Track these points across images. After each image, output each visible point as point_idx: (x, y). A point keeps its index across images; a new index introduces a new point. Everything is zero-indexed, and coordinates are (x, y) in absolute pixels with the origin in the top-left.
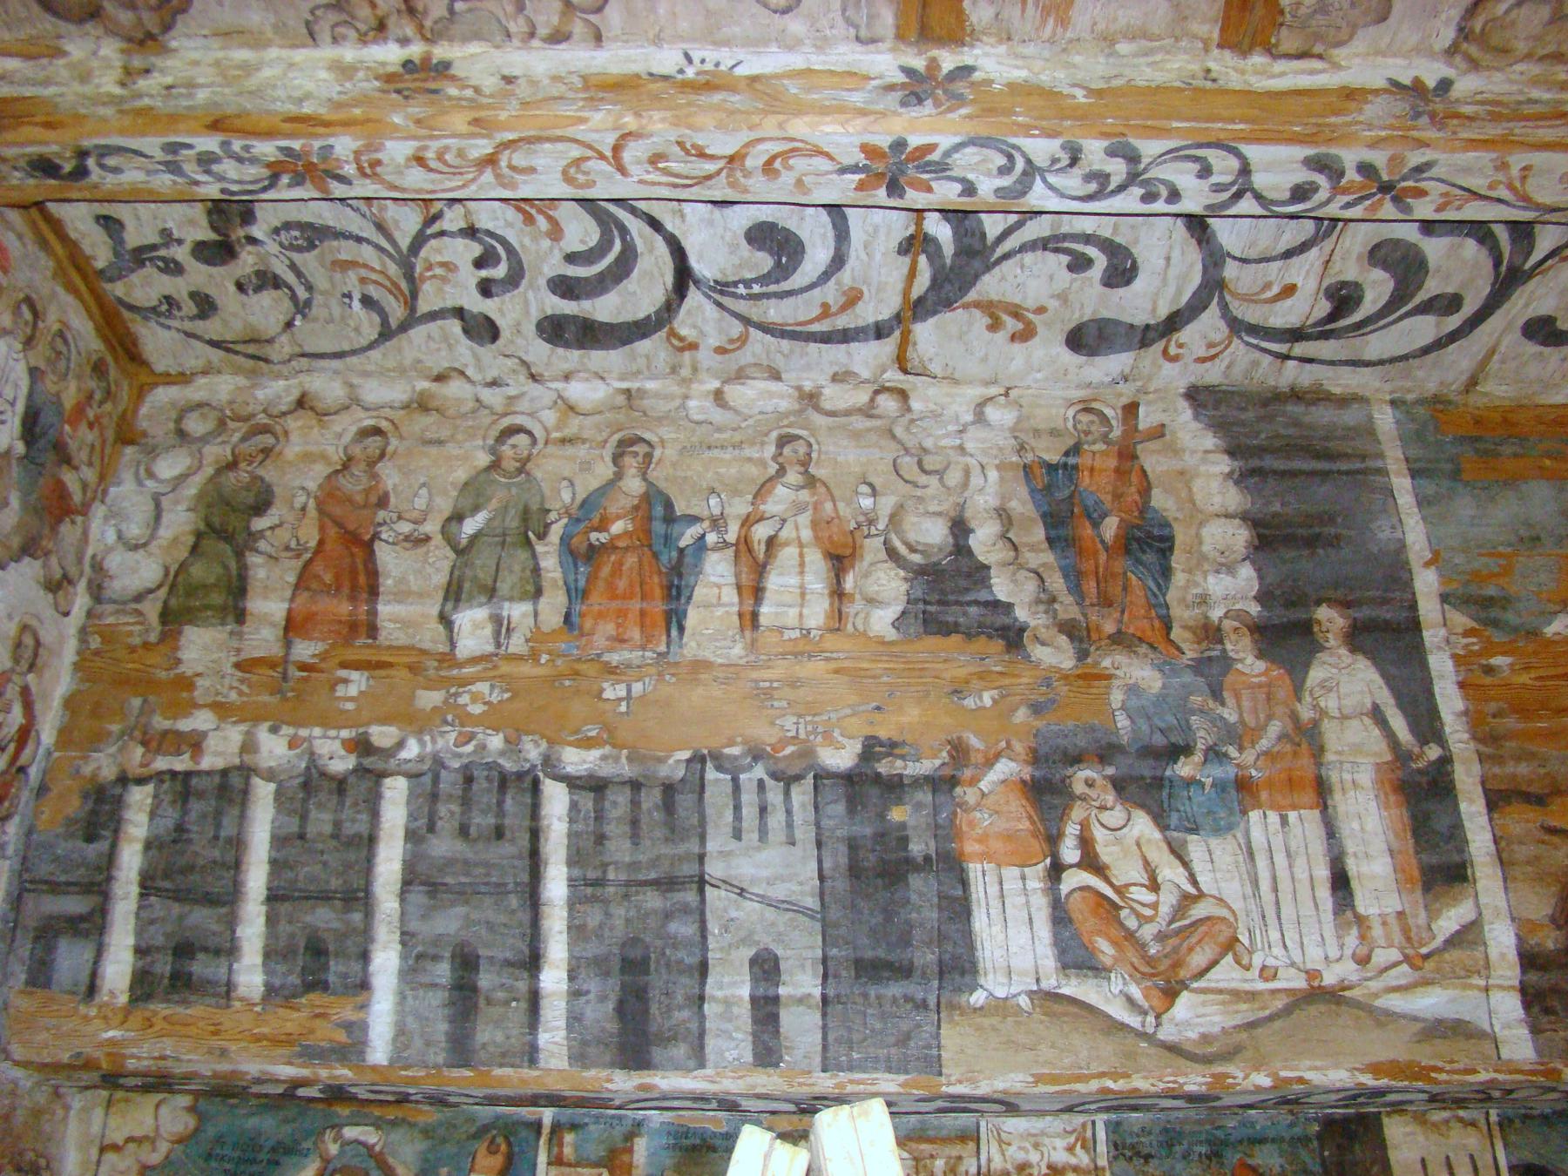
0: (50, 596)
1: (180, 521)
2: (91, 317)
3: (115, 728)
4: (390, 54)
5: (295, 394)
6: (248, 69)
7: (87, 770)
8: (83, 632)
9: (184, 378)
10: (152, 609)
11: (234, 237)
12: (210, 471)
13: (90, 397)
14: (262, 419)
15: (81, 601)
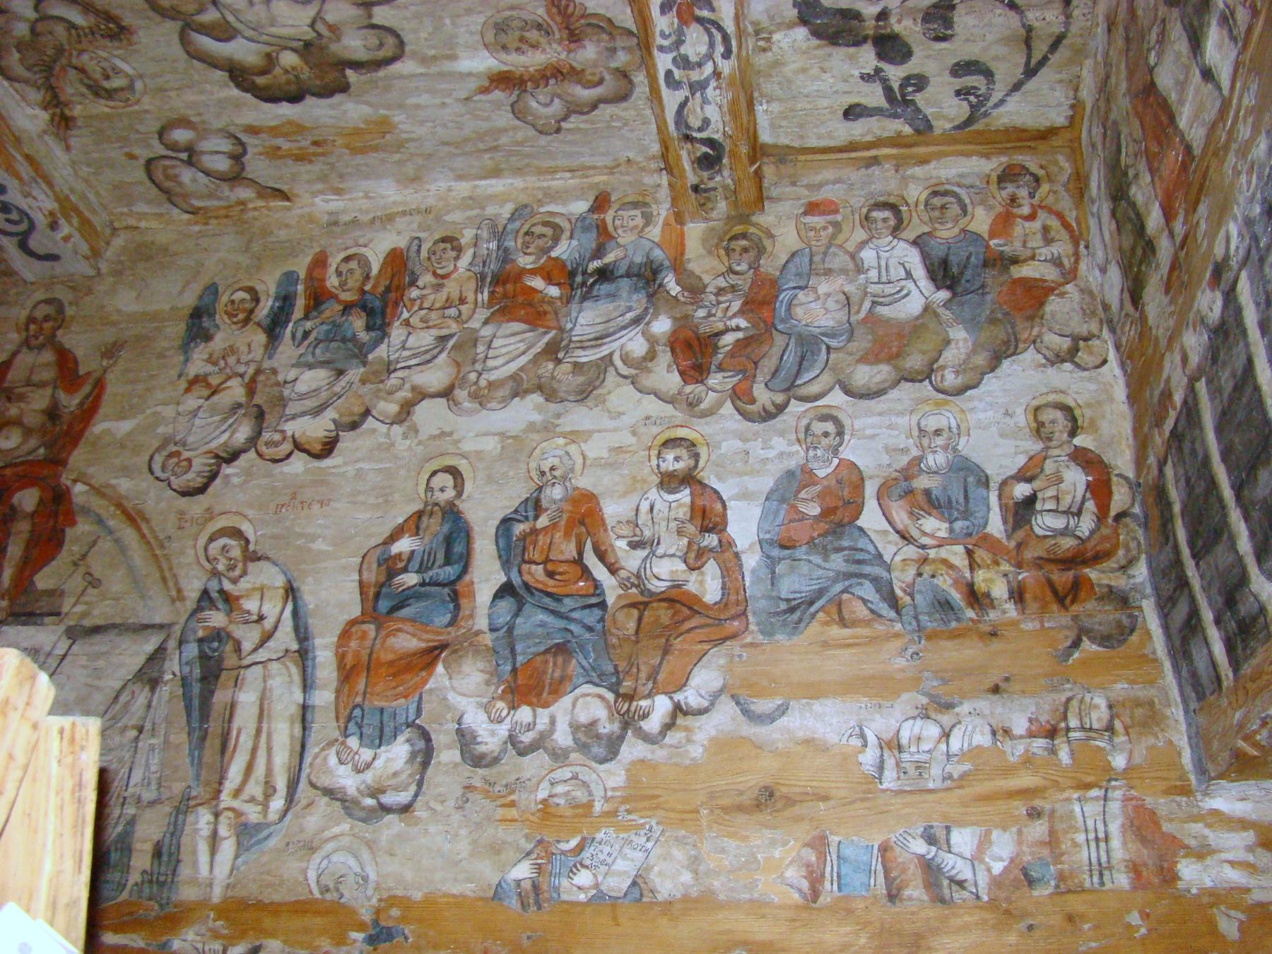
0: (1068, 366)
2: (968, 155)
8: (1122, 365)
11: (871, 32)
13: (1013, 199)
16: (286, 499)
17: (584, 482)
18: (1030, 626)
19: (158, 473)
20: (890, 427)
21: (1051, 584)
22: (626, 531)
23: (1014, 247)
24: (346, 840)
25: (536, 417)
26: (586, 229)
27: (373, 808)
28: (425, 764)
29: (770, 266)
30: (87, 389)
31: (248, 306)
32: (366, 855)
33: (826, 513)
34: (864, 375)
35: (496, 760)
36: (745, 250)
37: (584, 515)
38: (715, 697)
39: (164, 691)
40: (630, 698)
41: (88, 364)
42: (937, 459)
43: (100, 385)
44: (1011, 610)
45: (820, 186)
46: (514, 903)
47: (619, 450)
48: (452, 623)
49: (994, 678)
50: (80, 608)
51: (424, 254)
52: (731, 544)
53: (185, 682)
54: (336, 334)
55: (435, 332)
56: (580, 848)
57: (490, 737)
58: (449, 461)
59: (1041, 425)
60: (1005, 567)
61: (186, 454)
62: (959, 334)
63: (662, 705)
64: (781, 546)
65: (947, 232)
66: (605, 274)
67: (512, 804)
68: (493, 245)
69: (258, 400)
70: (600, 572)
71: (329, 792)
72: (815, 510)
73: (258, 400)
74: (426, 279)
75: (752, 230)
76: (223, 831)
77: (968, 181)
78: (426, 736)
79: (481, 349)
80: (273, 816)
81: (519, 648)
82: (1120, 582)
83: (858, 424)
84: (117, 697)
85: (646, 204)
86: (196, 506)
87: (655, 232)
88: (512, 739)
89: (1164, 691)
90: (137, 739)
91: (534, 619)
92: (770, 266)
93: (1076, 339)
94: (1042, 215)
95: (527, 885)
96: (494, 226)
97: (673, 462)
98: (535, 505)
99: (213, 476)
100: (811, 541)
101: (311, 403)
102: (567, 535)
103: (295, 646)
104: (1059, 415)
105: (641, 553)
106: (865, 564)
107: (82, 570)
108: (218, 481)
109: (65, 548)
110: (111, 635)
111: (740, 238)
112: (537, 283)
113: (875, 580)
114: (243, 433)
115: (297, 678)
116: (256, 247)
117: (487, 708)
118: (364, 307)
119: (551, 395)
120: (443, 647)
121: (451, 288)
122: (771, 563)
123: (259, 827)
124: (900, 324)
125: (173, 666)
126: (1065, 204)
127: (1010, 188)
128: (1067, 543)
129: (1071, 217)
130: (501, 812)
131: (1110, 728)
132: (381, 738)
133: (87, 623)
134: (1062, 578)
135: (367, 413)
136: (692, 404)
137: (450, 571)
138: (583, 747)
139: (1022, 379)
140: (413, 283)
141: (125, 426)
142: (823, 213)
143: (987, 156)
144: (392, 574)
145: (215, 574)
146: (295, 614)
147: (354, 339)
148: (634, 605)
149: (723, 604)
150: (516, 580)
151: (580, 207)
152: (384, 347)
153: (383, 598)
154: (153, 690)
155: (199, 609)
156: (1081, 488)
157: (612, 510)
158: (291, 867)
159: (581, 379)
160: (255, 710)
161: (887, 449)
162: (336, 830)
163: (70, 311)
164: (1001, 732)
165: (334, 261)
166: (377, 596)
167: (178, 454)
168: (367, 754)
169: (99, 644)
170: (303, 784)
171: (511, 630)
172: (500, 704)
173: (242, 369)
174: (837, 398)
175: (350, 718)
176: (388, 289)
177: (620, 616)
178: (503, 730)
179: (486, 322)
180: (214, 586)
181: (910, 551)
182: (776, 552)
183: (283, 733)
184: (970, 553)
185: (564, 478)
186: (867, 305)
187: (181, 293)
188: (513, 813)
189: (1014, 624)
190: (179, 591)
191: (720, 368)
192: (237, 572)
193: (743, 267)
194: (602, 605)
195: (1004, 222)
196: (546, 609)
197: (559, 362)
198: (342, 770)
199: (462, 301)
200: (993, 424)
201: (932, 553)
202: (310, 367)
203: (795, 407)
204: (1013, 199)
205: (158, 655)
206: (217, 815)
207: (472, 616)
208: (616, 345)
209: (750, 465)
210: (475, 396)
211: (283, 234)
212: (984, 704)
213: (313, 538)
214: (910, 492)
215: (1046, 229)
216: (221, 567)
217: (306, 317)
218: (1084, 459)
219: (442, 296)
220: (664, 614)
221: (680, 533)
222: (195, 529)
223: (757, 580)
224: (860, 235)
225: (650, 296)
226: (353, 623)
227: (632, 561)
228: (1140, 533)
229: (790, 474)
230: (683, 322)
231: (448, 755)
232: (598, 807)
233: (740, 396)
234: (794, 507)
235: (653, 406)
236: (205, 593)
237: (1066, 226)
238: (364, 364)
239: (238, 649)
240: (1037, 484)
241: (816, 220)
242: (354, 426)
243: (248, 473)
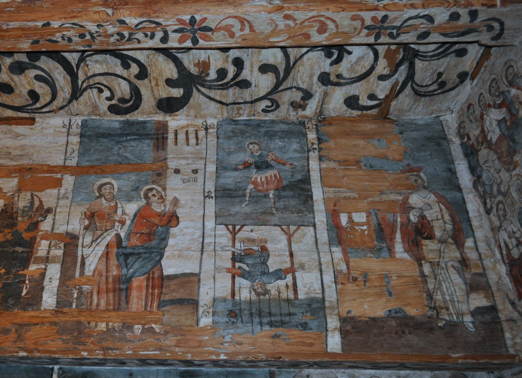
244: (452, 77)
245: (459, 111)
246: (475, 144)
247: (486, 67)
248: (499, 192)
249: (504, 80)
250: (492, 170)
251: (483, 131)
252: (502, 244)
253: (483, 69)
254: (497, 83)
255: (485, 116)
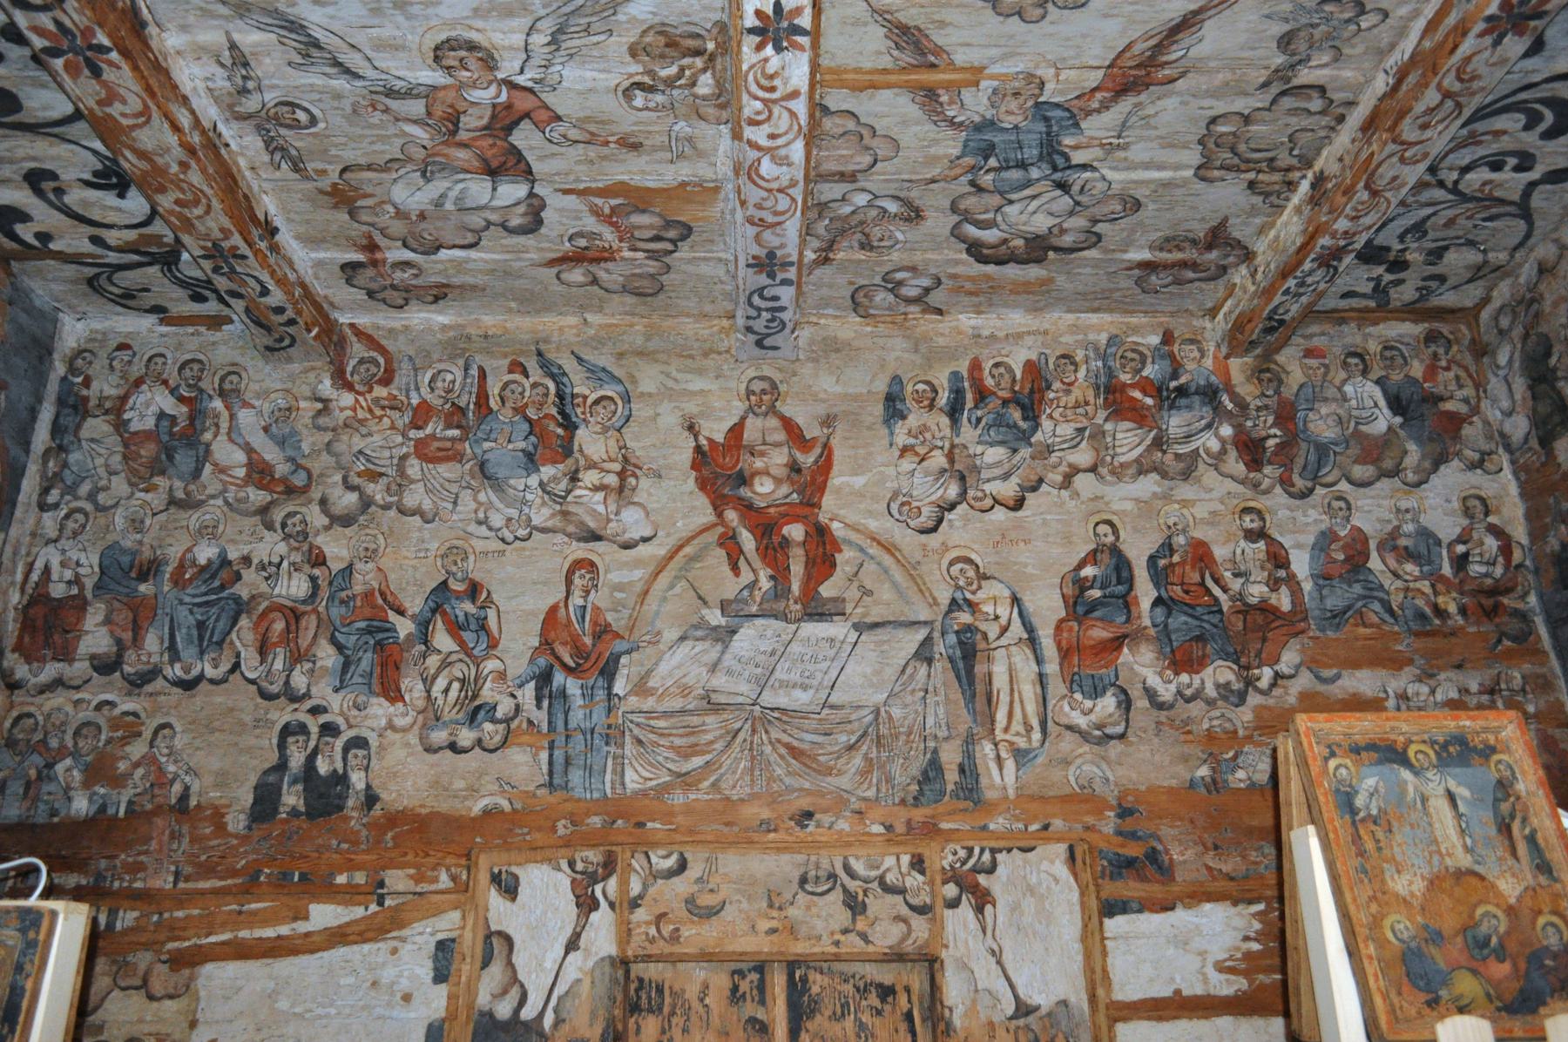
0: (1479, 471)
1: (1520, 385)
2: (1404, 320)
3: (1548, 520)
4: (1305, 186)
5: (1536, 266)
6: (1277, 238)
7: (1548, 550)
8: (1515, 473)
9: (1486, 300)
10: (1534, 443)
12: (1519, 346)
13: (1435, 356)
14: (1528, 296)
15: (1504, 459)
16: (999, 538)
17: (1198, 534)
18: (1472, 629)
19: (897, 516)
20: (1379, 506)
21: (1481, 606)
22: (1229, 566)
23: (1439, 390)
24: (1089, 757)
25: (1159, 490)
26: (1162, 357)
27: (1101, 737)
28: (1128, 709)
29: (1289, 392)
30: (818, 450)
31: (930, 395)
32: (1104, 766)
33: (1347, 560)
34: (1359, 471)
35: (1172, 706)
36: (1270, 380)
37: (1201, 554)
38: (1298, 667)
39: (938, 665)
40: (1248, 668)
41: (812, 431)
42: (1409, 528)
43: (826, 446)
44: (1460, 621)
45: (1312, 336)
46: (1203, 790)
47: (1214, 513)
48: (1128, 620)
49: (1456, 659)
50: (859, 610)
51: (1051, 366)
52: (1294, 576)
53: (951, 660)
54: (999, 422)
55: (1073, 425)
56: (1235, 757)
57: (1166, 692)
58: (1105, 517)
59: (1467, 508)
60: (1454, 595)
61: (915, 504)
62: (1412, 447)
63: (1267, 673)
64: (1323, 578)
65: (1396, 376)
66: (1182, 391)
67: (1189, 732)
68: (1100, 364)
69: (957, 467)
70: (1217, 591)
71: (1069, 728)
72: (1342, 557)
73: (957, 467)
74: (1057, 385)
75: (1272, 366)
76: (1004, 754)
77: (1406, 340)
78: (1124, 692)
79: (1109, 439)
80: (1035, 744)
81: (1173, 637)
82: (1520, 606)
83: (1359, 503)
84: (903, 671)
85: (1199, 342)
86: (933, 540)
87: (1209, 362)
88: (1179, 693)
89: (1552, 670)
90: (924, 698)
91: (1179, 620)
92: (1289, 392)
93: (1483, 453)
94: (1454, 367)
95: (1208, 780)
96: (1096, 349)
97: (1249, 522)
98: (1168, 547)
99: (940, 521)
100: (1340, 576)
101: (997, 472)
102: (1193, 567)
103: (1025, 636)
104: (1477, 503)
105: (1241, 580)
106: (1373, 590)
107: (856, 584)
108: (944, 524)
109: (838, 568)
110: (889, 629)
111: (1266, 372)
112: (1137, 394)
113: (1381, 601)
114: (953, 491)
115: (1031, 656)
116: (923, 348)
117: (1160, 674)
118: (1018, 404)
119: (1164, 475)
120: (1125, 636)
121: (1077, 393)
122: (1319, 588)
123: (1027, 752)
124: (1375, 438)
125: (940, 648)
126: (1468, 359)
127: (1433, 348)
128: (1489, 581)
129: (1473, 369)
130: (1183, 737)
131: (1523, 690)
132: (1096, 692)
133: (868, 620)
134: (1488, 602)
135: (1041, 481)
136: (1256, 486)
137: (1121, 589)
138: (1225, 698)
139: (1452, 479)
140: (1049, 387)
141: (859, 481)
142: (1317, 357)
143: (1416, 322)
144: (1083, 589)
145: (958, 587)
146: (1021, 614)
147: (1015, 426)
148: (1238, 612)
149: (1293, 612)
150: (1164, 594)
151: (1155, 340)
152: (1039, 433)
153: (1078, 605)
154: (930, 665)
155: (950, 611)
156: (1495, 549)
157: (1220, 552)
158: (1056, 774)
159: (1182, 465)
160: (1006, 677)
161: (1379, 520)
162: (1081, 751)
163: (783, 388)
164: (1464, 691)
165: (987, 366)
166: (1075, 603)
167: (909, 503)
168: (1088, 704)
169: (881, 634)
170: (1050, 723)
171: (1166, 626)
172: (1168, 672)
173: (940, 444)
174: (1344, 486)
175: (1073, 682)
176: (1032, 391)
177: (1233, 619)
178: (1173, 688)
179: (1106, 420)
180: (958, 595)
181: (1399, 584)
182: (1321, 582)
183: (1029, 691)
184: (1433, 586)
185: (1184, 531)
186: (1352, 424)
187: (872, 381)
188: (1190, 737)
189: (1462, 628)
190: (934, 599)
191: (1270, 463)
192: (974, 587)
193: (1270, 392)
194: (1220, 611)
195: (1431, 371)
196: (1186, 614)
197: (1164, 452)
198: (1074, 714)
199: (1087, 403)
200: (1439, 504)
201: (1411, 585)
202: (992, 445)
203: (1320, 491)
204: (1435, 356)
205: (927, 641)
206: (996, 745)
207: (1139, 617)
208: (1199, 443)
209: (1300, 527)
210: (1113, 473)
211: (941, 341)
212: (1451, 674)
213: (1026, 566)
214: (1395, 548)
215: (1457, 378)
216: (961, 583)
217: (976, 407)
218: (1495, 531)
219: (1071, 400)
220: (1260, 619)
221: (1262, 568)
222: (936, 557)
223: (1312, 599)
224: (1343, 375)
225: (1215, 409)
226: (1062, 621)
227: (1236, 585)
228: (1530, 577)
229: (1323, 533)
230: (1239, 428)
231: (1141, 703)
232: (1241, 733)
233: (1286, 482)
234: (1328, 555)
235: (1231, 486)
236: (954, 601)
237: (1470, 376)
238: (1031, 445)
239: (985, 636)
240: (1469, 545)
241: (1313, 362)
242: (1034, 489)
243: (966, 520)
244: (149, 300)
245: (97, 332)
246: (92, 403)
247: (198, 334)
248: (91, 497)
249: (217, 380)
250: (99, 461)
251: (124, 399)
252: (39, 565)
253: (190, 330)
254: (202, 370)
255: (144, 387)
